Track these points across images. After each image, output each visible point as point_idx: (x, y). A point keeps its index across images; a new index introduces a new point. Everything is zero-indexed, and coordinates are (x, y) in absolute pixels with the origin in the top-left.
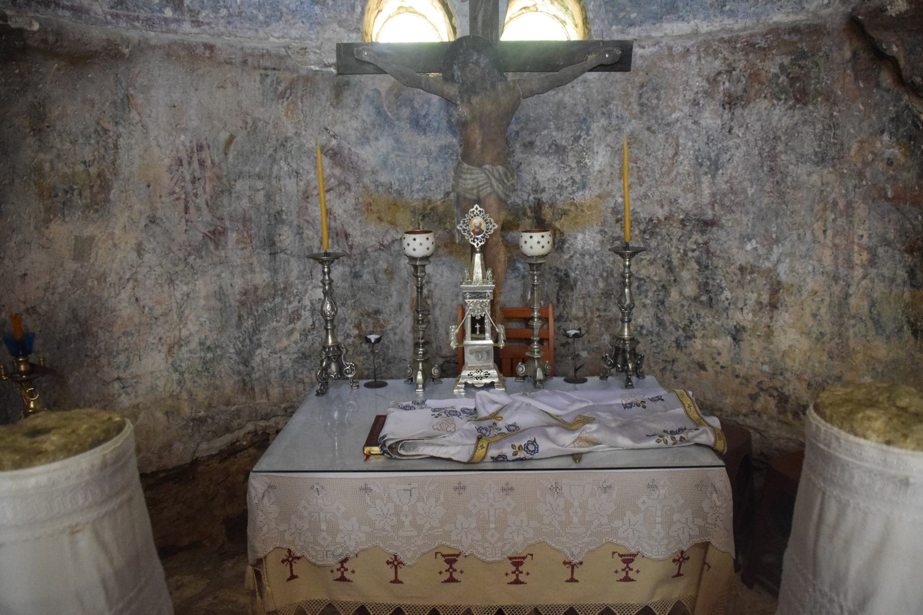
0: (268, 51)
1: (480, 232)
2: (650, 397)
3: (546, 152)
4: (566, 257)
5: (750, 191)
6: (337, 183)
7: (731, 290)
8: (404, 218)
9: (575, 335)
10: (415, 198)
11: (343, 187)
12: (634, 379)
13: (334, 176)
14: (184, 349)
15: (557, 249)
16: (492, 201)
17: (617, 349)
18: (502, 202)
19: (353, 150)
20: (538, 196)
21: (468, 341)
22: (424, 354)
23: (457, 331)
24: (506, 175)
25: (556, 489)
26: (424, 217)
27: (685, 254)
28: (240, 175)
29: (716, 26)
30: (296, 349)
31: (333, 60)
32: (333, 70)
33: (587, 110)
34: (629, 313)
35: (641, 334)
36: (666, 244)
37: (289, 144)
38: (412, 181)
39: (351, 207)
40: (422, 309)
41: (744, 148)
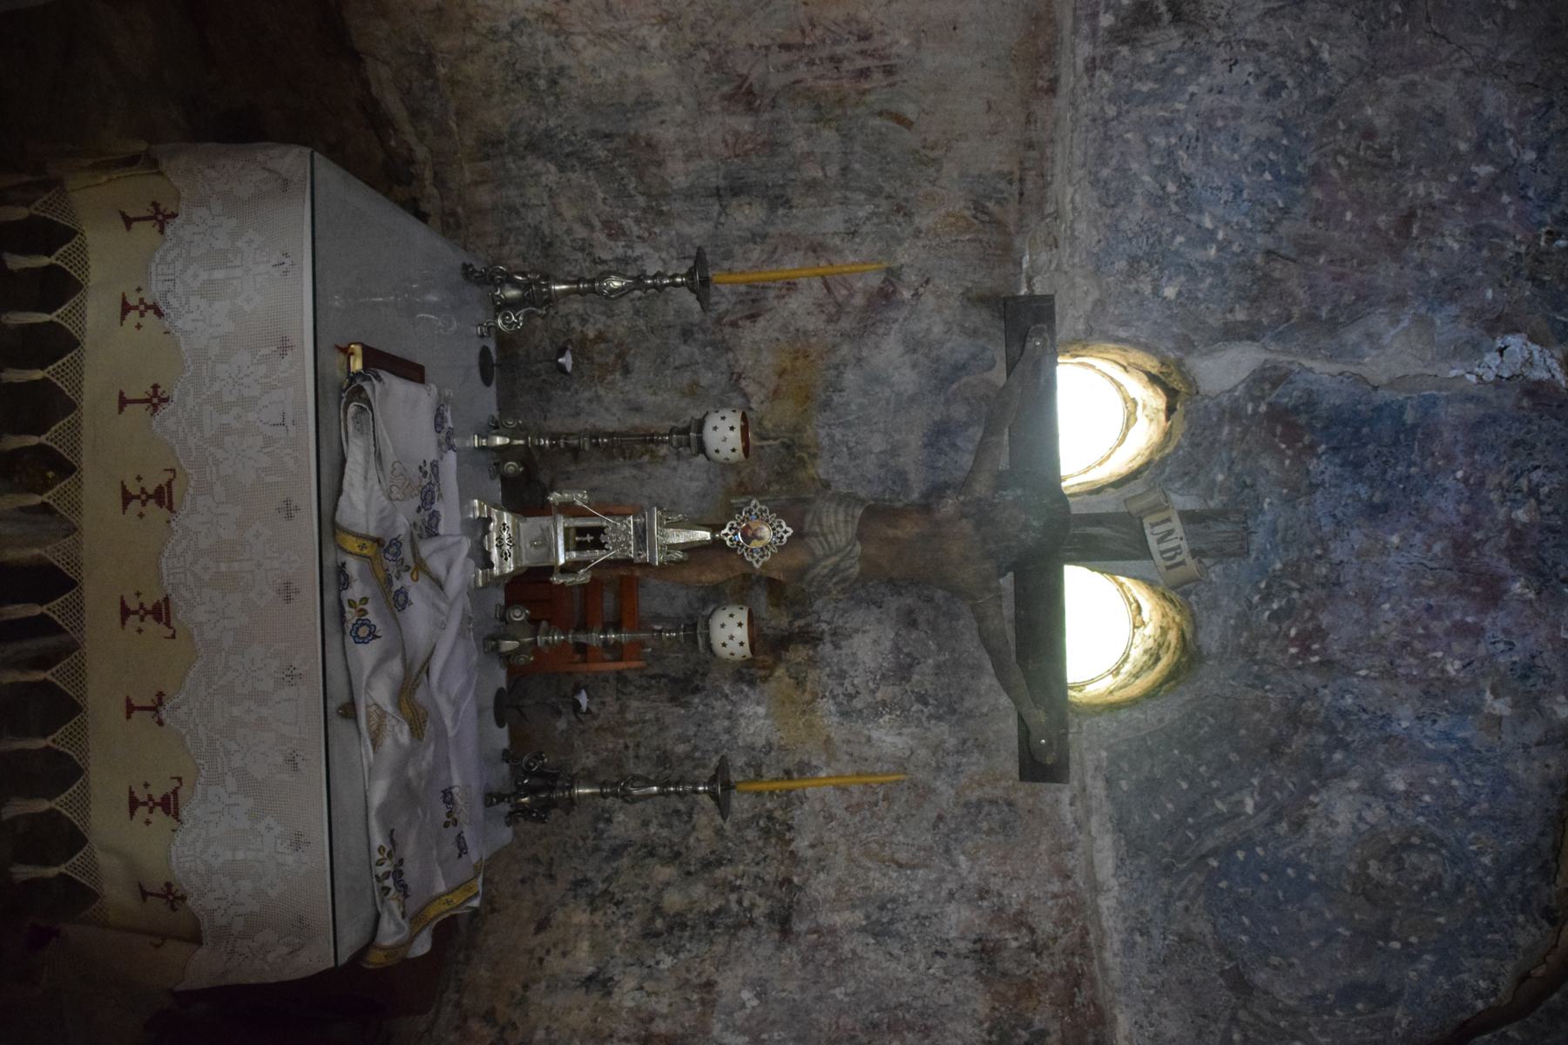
0: (1051, 183)
1: (747, 539)
2: (465, 835)
3: (899, 650)
4: (727, 689)
5: (839, 993)
6: (840, 299)
7: (673, 969)
8: (780, 415)
9: (577, 705)
10: (819, 431)
11: (833, 310)
12: (505, 808)
13: (851, 296)
14: (552, 40)
15: (739, 671)
16: (799, 558)
17: (555, 777)
18: (802, 572)
19: (896, 326)
20: (827, 638)
21: (562, 523)
22: (540, 448)
23: (579, 503)
24: (844, 580)
25: (291, 676)
26: (788, 447)
27: (734, 889)
28: (847, 138)
29: (1108, 922)
30: (559, 233)
31: (1038, 291)
32: (1023, 291)
33: (969, 715)
34: (616, 795)
35: (597, 819)
36: (750, 856)
37: (900, 219)
38: (847, 425)
39: (800, 324)
40: (632, 446)
41: (910, 977)
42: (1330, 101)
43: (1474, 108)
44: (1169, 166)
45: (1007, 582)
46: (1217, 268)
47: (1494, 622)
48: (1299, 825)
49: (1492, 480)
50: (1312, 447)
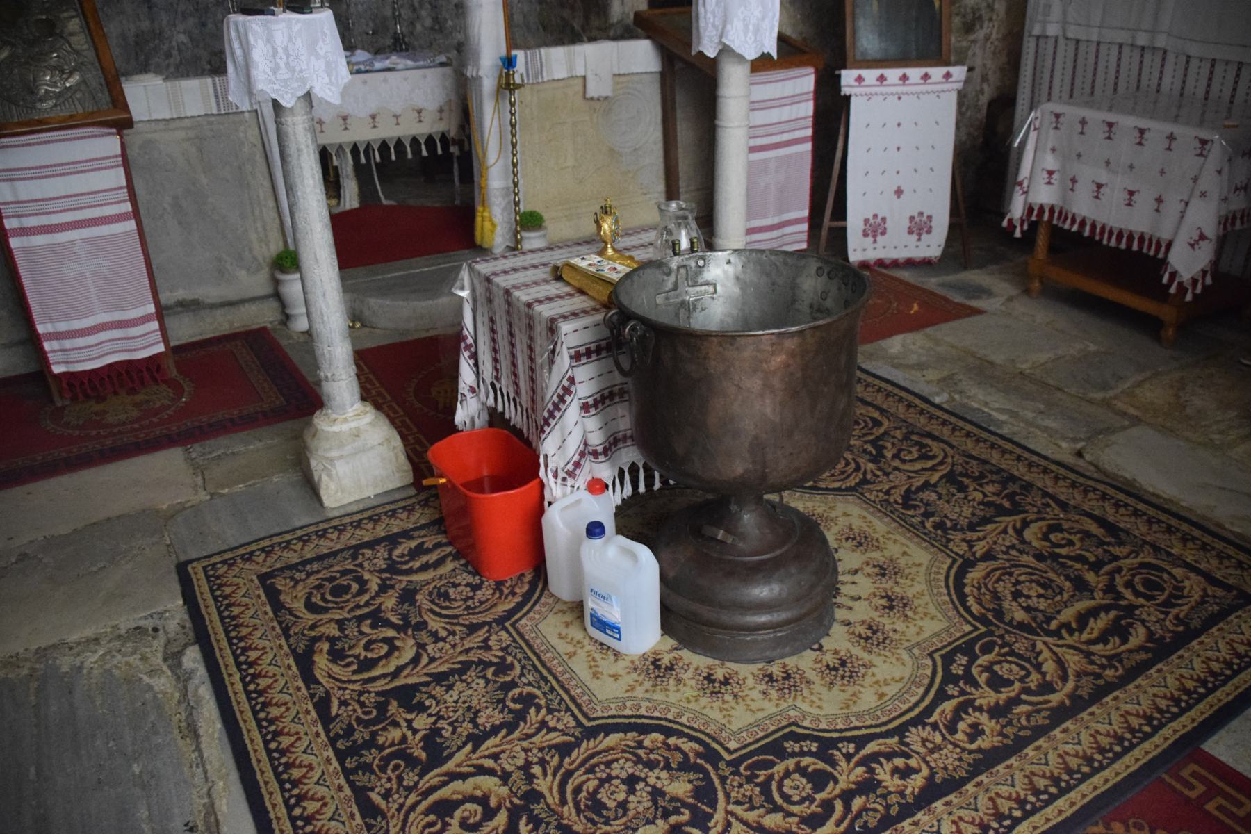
25: (385, 80)
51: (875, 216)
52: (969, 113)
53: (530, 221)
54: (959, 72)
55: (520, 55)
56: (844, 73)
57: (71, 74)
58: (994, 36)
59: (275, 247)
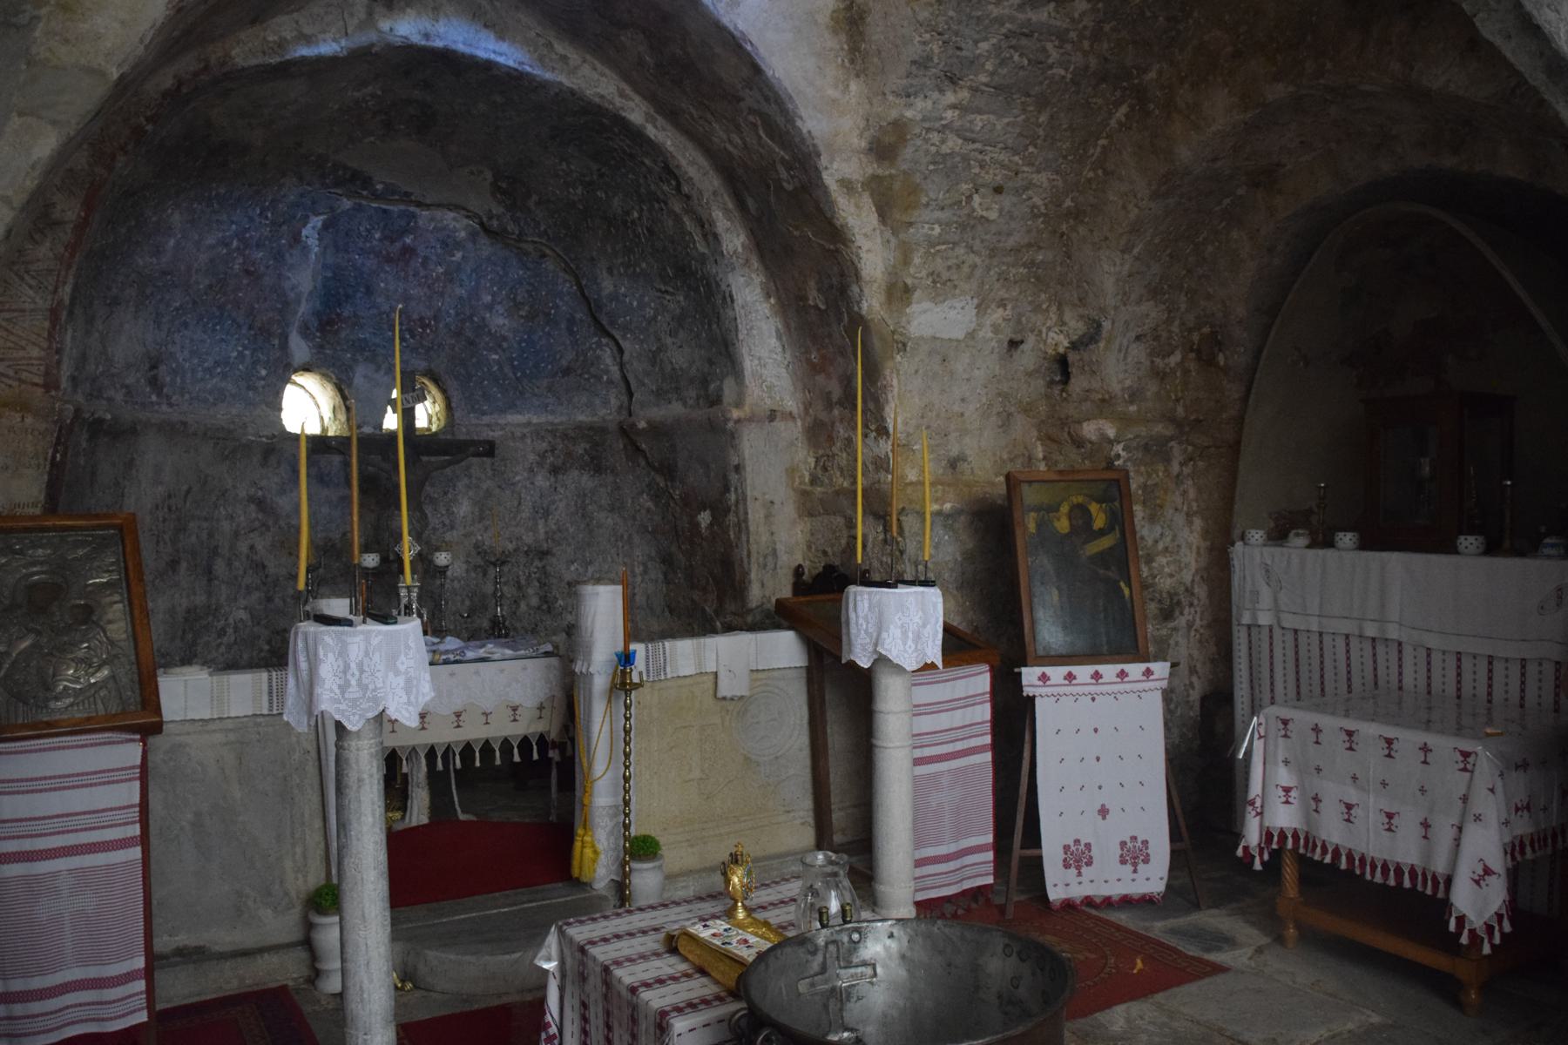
25: (477, 673)
29: (543, 419)
42: (195, 303)
43: (212, 247)
44: (209, 370)
45: (425, 459)
46: (255, 350)
47: (422, 251)
48: (505, 338)
49: (361, 245)
50: (338, 315)
51: (1077, 842)
52: (1179, 712)
53: (642, 849)
54: (1161, 669)
55: (638, 648)
56: (1024, 670)
57: (99, 668)
58: (1198, 622)
59: (314, 878)
